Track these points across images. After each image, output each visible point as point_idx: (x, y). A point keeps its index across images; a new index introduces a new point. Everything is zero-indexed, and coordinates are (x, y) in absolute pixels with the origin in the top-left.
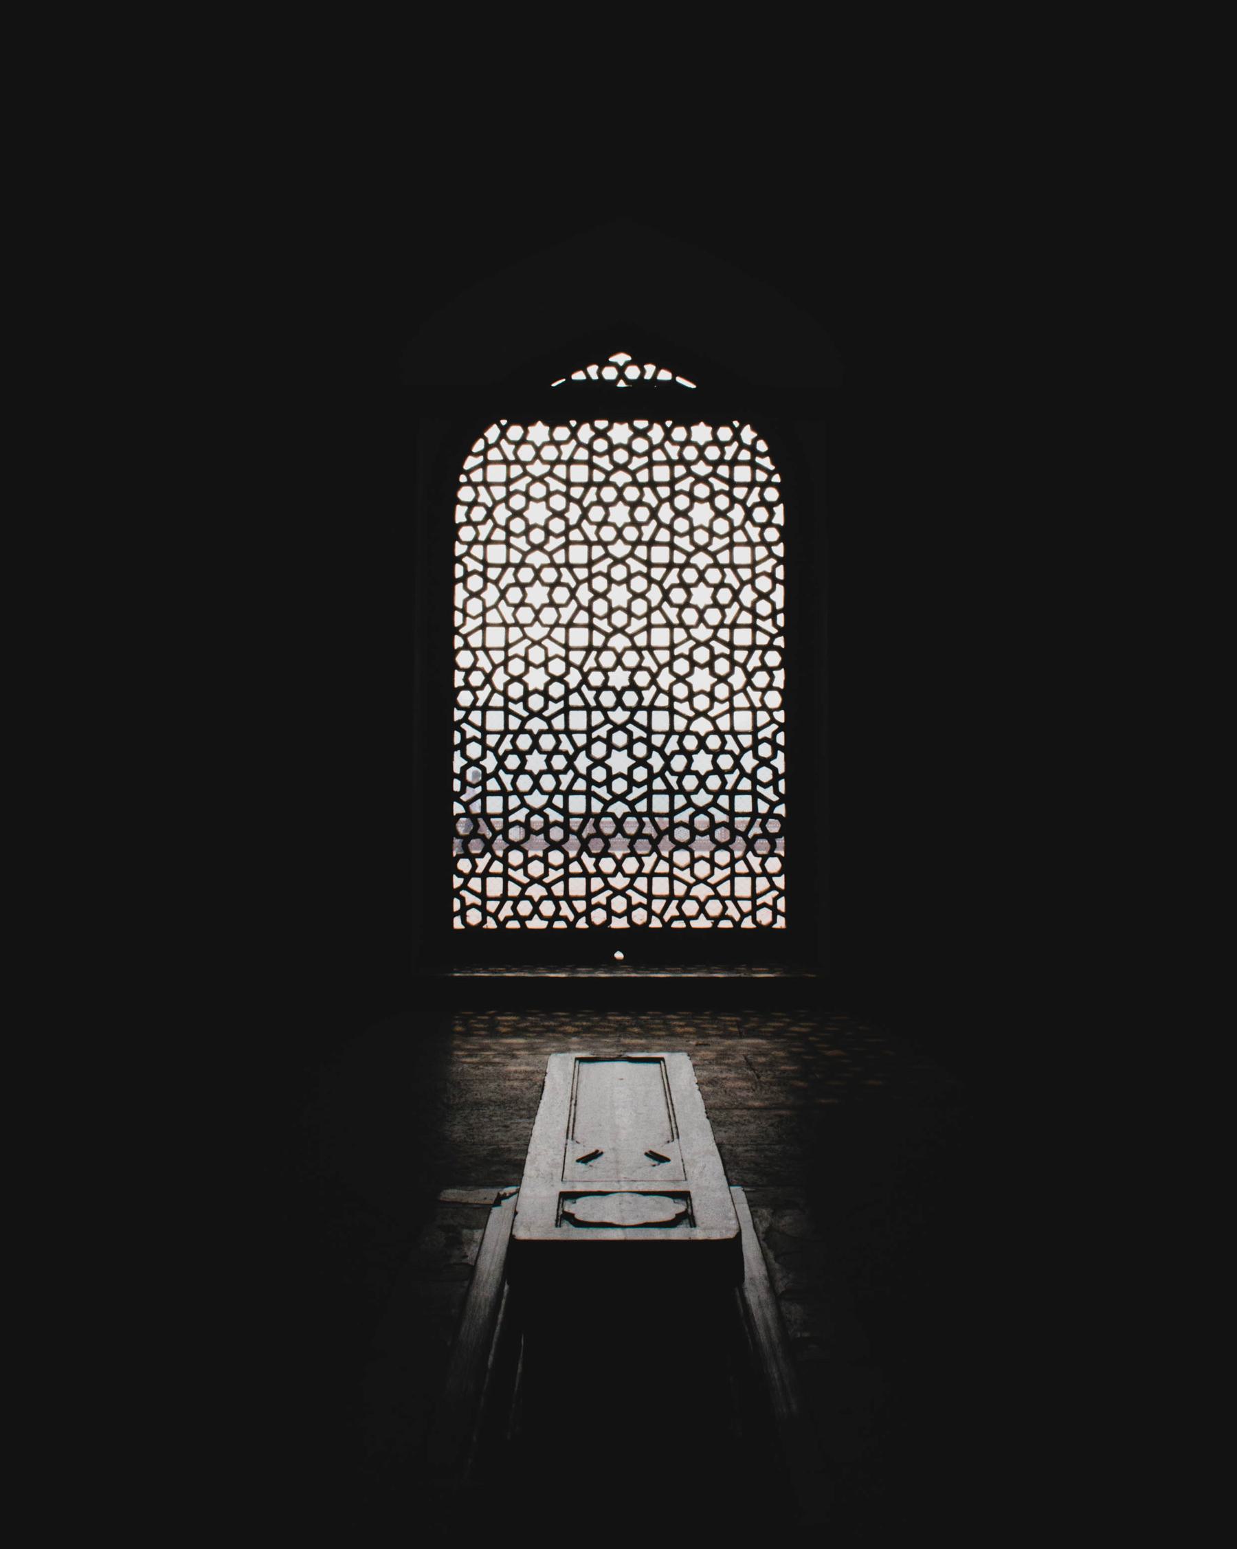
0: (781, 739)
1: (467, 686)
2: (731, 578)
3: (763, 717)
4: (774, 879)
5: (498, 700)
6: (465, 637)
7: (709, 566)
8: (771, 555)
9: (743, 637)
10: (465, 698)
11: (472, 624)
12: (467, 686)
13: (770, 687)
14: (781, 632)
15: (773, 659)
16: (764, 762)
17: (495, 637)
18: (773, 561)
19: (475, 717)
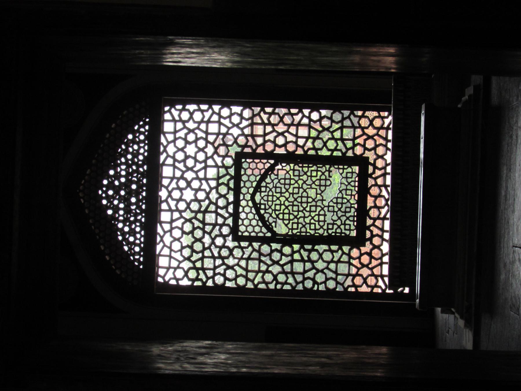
0: (269, 110)
1: (235, 279)
2: (182, 134)
3: (257, 120)
4: (345, 116)
5: (243, 263)
6: (208, 278)
7: (175, 146)
8: (169, 111)
9: (213, 128)
10: (241, 281)
11: (202, 276)
12: (235, 279)
13: (241, 115)
14: (210, 107)
15: (225, 112)
16: (281, 119)
17: (208, 263)
18: (173, 110)
19: (251, 275)
